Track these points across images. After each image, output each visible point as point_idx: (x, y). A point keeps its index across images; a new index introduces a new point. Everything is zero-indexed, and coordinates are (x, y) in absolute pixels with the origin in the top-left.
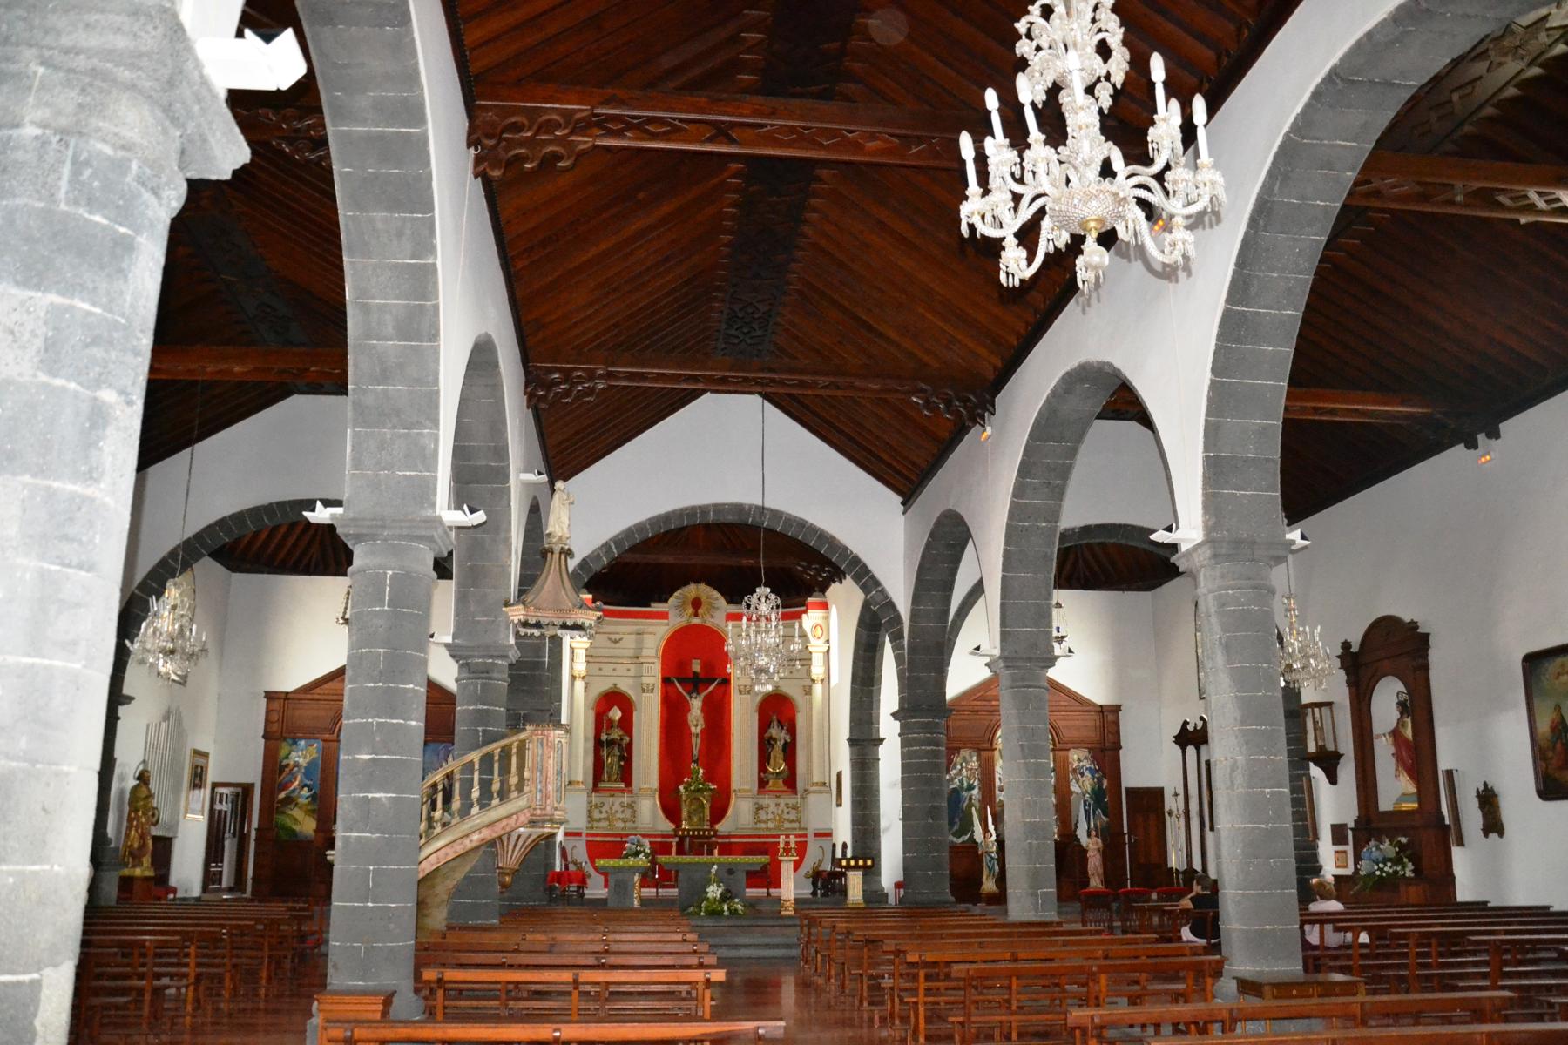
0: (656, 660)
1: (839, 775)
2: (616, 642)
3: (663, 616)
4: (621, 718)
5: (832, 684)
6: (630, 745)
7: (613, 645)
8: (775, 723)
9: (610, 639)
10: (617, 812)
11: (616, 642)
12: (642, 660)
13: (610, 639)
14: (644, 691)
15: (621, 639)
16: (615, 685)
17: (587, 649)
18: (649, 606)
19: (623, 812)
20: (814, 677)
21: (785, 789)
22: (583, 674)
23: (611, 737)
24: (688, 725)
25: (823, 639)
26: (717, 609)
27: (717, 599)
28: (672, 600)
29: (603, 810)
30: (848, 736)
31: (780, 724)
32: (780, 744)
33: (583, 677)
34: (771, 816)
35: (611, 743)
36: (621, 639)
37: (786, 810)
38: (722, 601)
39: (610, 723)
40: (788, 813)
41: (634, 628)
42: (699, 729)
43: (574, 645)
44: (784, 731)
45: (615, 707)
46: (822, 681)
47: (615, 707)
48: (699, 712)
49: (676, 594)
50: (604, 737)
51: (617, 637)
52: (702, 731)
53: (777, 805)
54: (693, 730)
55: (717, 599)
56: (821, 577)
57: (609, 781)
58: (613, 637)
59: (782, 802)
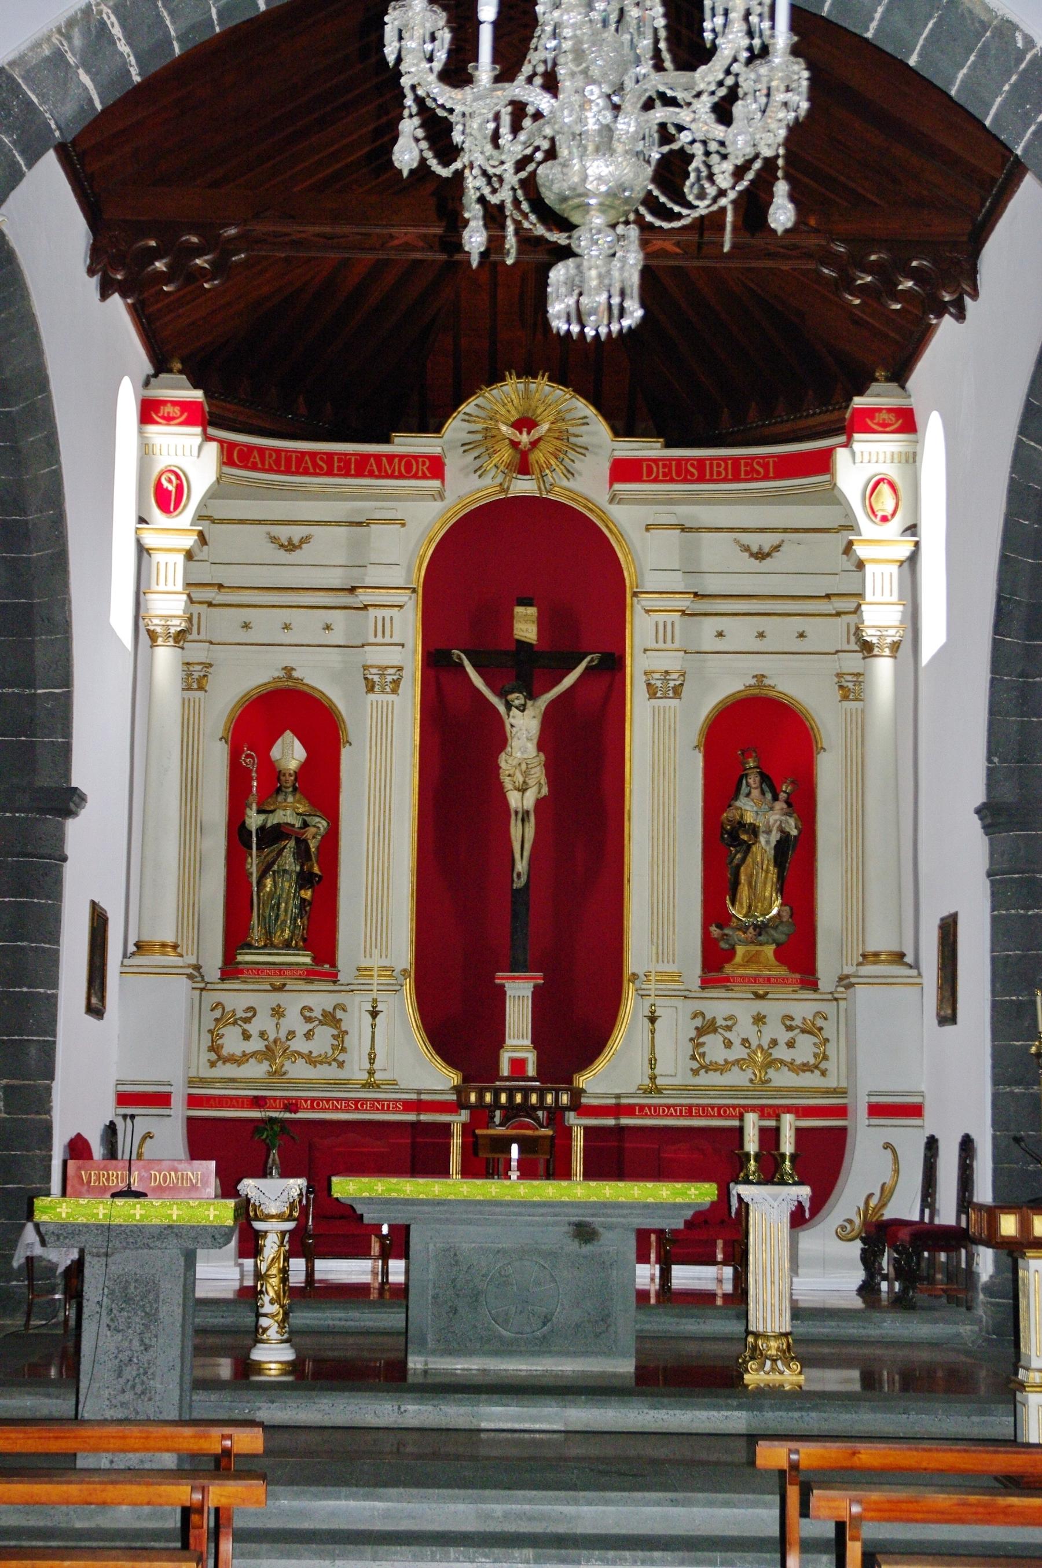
0: (402, 597)
1: (948, 930)
2: (290, 547)
3: (435, 467)
4: (304, 766)
5: (927, 652)
6: (331, 840)
7: (283, 556)
8: (753, 780)
9: (274, 539)
10: (291, 1034)
11: (290, 547)
12: (364, 597)
13: (274, 539)
14: (371, 687)
15: (305, 540)
16: (289, 670)
17: (189, 555)
18: (387, 440)
19: (309, 1035)
20: (870, 635)
21: (782, 971)
22: (177, 625)
23: (274, 820)
24: (500, 785)
25: (896, 525)
26: (583, 450)
27: (584, 422)
28: (455, 428)
29: (253, 1028)
30: (979, 797)
31: (769, 783)
32: (766, 845)
33: (180, 637)
34: (739, 1052)
35: (272, 835)
36: (305, 540)
37: (784, 1036)
38: (599, 429)
39: (272, 775)
40: (791, 1044)
41: (340, 509)
42: (529, 800)
43: (150, 540)
44: (780, 805)
45: (288, 735)
46: (895, 647)
47: (288, 735)
48: (531, 748)
49: (464, 408)
50: (254, 820)
51: (296, 533)
52: (539, 803)
53: (759, 1019)
54: (514, 799)
55: (584, 422)
56: (897, 296)
57: (269, 945)
58: (284, 533)
59: (773, 1009)
